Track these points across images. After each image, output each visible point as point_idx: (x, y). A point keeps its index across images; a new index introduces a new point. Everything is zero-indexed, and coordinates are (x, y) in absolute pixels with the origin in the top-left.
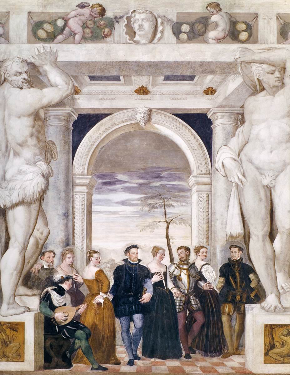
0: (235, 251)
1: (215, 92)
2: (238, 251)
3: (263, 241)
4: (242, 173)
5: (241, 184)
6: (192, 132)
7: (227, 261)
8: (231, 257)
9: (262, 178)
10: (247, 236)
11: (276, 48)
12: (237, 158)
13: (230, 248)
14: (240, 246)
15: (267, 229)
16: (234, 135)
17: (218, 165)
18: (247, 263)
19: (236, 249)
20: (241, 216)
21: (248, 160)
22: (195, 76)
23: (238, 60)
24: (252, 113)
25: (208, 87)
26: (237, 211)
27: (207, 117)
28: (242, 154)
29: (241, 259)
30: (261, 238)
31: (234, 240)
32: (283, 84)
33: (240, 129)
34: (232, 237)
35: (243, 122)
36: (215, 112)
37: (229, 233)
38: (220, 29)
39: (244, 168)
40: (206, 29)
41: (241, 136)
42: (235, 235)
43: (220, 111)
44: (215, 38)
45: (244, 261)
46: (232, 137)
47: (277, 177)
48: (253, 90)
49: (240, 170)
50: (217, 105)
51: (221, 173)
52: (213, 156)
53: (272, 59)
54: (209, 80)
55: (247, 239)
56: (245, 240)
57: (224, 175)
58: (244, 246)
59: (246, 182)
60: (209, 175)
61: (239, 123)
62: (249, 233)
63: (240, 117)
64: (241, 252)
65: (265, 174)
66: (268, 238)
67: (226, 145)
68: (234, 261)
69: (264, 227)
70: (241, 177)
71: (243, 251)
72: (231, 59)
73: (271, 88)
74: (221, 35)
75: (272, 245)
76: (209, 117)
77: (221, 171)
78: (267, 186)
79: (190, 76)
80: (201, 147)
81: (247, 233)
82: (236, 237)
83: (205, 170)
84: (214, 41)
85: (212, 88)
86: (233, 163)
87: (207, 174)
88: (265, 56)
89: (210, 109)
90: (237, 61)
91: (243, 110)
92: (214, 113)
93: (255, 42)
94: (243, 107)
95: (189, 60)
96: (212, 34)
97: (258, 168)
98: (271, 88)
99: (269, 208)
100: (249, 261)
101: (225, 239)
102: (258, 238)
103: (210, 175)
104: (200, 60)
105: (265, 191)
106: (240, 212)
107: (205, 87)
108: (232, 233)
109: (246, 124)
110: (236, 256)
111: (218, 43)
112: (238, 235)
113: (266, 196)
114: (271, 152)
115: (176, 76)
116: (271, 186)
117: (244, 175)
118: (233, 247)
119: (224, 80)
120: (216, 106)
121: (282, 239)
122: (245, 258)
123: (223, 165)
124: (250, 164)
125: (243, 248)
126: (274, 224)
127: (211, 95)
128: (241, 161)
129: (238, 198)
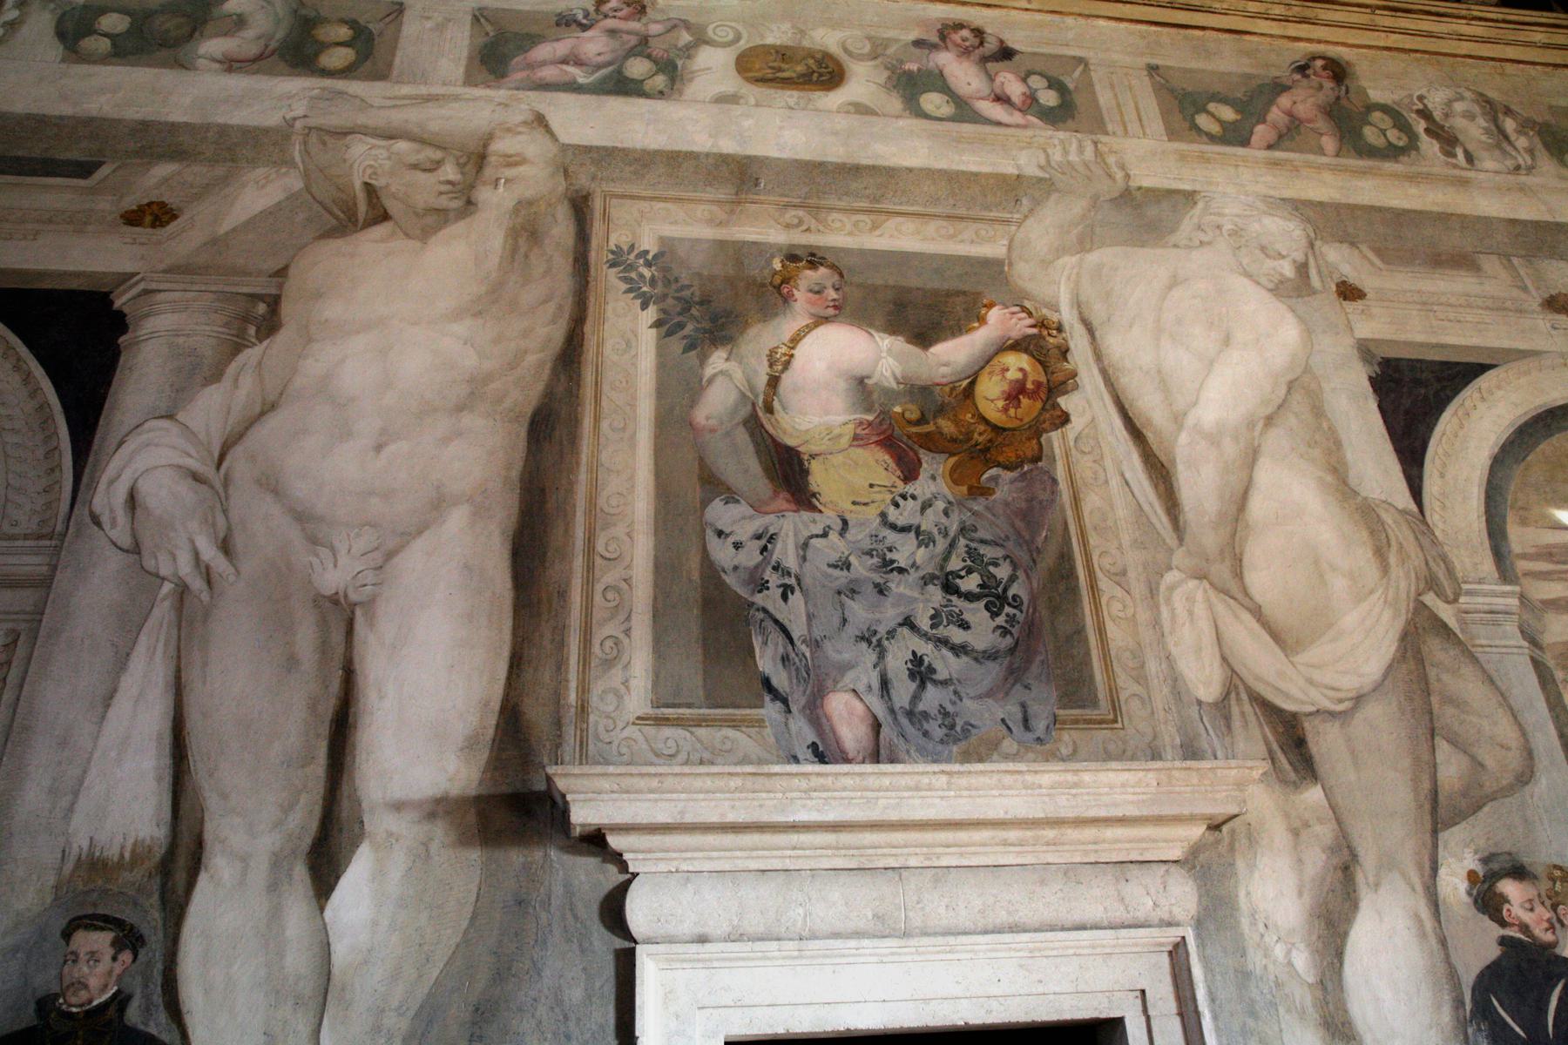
0: (92, 953)
1: (175, 217)
2: (110, 952)
3: (273, 887)
4: (222, 535)
5: (205, 587)
6: (19, 359)
7: (28, 1018)
8: (56, 989)
9: (315, 561)
10: (182, 861)
11: (457, 98)
12: (208, 470)
13: (67, 935)
14: (128, 915)
15: (304, 819)
16: (216, 376)
17: (108, 497)
18: (153, 1030)
19: (101, 940)
20: (167, 750)
21: (259, 482)
22: (100, 164)
23: (298, 125)
24: (318, 295)
25: (146, 201)
26: (152, 719)
27: (112, 303)
28: (238, 452)
29: (121, 1001)
30: (260, 871)
31: (100, 882)
32: (469, 202)
33: (251, 355)
34: (94, 865)
35: (270, 325)
36: (154, 286)
37: (81, 842)
38: (249, 33)
39: (234, 514)
40: (194, 30)
41: (247, 382)
42: (113, 853)
43: (174, 286)
44: (220, 57)
45: (133, 1015)
46: (204, 385)
47: (390, 555)
48: (337, 218)
49: (214, 525)
50: (168, 262)
51: (113, 534)
52: (91, 459)
53: (434, 126)
54: (156, 180)
55: (180, 877)
56: (163, 885)
57: (126, 541)
58: (150, 920)
59: (232, 578)
60: (48, 543)
61: (252, 330)
62: (199, 844)
63: (262, 308)
64: (126, 956)
65: (337, 544)
66: (301, 872)
67: (170, 416)
68: (70, 1015)
69: (287, 809)
70: (209, 552)
71: (142, 952)
72: (273, 119)
73: (416, 214)
74: (253, 50)
75: (322, 909)
76: (117, 304)
77: (114, 523)
78: (334, 600)
79: (79, 164)
80: (47, 421)
81: (186, 839)
82: (120, 864)
83: (36, 519)
84: (217, 66)
85: (162, 205)
86: (185, 489)
87: (40, 537)
88: (411, 116)
89: (133, 275)
90: (292, 126)
91: (281, 286)
92: (146, 292)
93: (382, 75)
94: (282, 273)
95: (94, 113)
96: (214, 46)
97: (302, 517)
98: (416, 214)
99: (328, 707)
100: (162, 1016)
101: (51, 880)
102: (244, 873)
103: (54, 543)
104: (138, 117)
105: (323, 623)
106: (167, 726)
107: (130, 202)
108: (102, 838)
109: (282, 337)
110: (94, 983)
111: (230, 70)
112: (133, 851)
113: (324, 648)
114: (379, 448)
115: (18, 159)
116: (353, 597)
117: (226, 547)
118: (88, 927)
119: (225, 180)
120: (162, 266)
121: (379, 874)
122: (147, 997)
123: (132, 500)
124: (269, 498)
125: (145, 930)
126: (345, 789)
127: (153, 226)
128: (227, 482)
129: (172, 651)
